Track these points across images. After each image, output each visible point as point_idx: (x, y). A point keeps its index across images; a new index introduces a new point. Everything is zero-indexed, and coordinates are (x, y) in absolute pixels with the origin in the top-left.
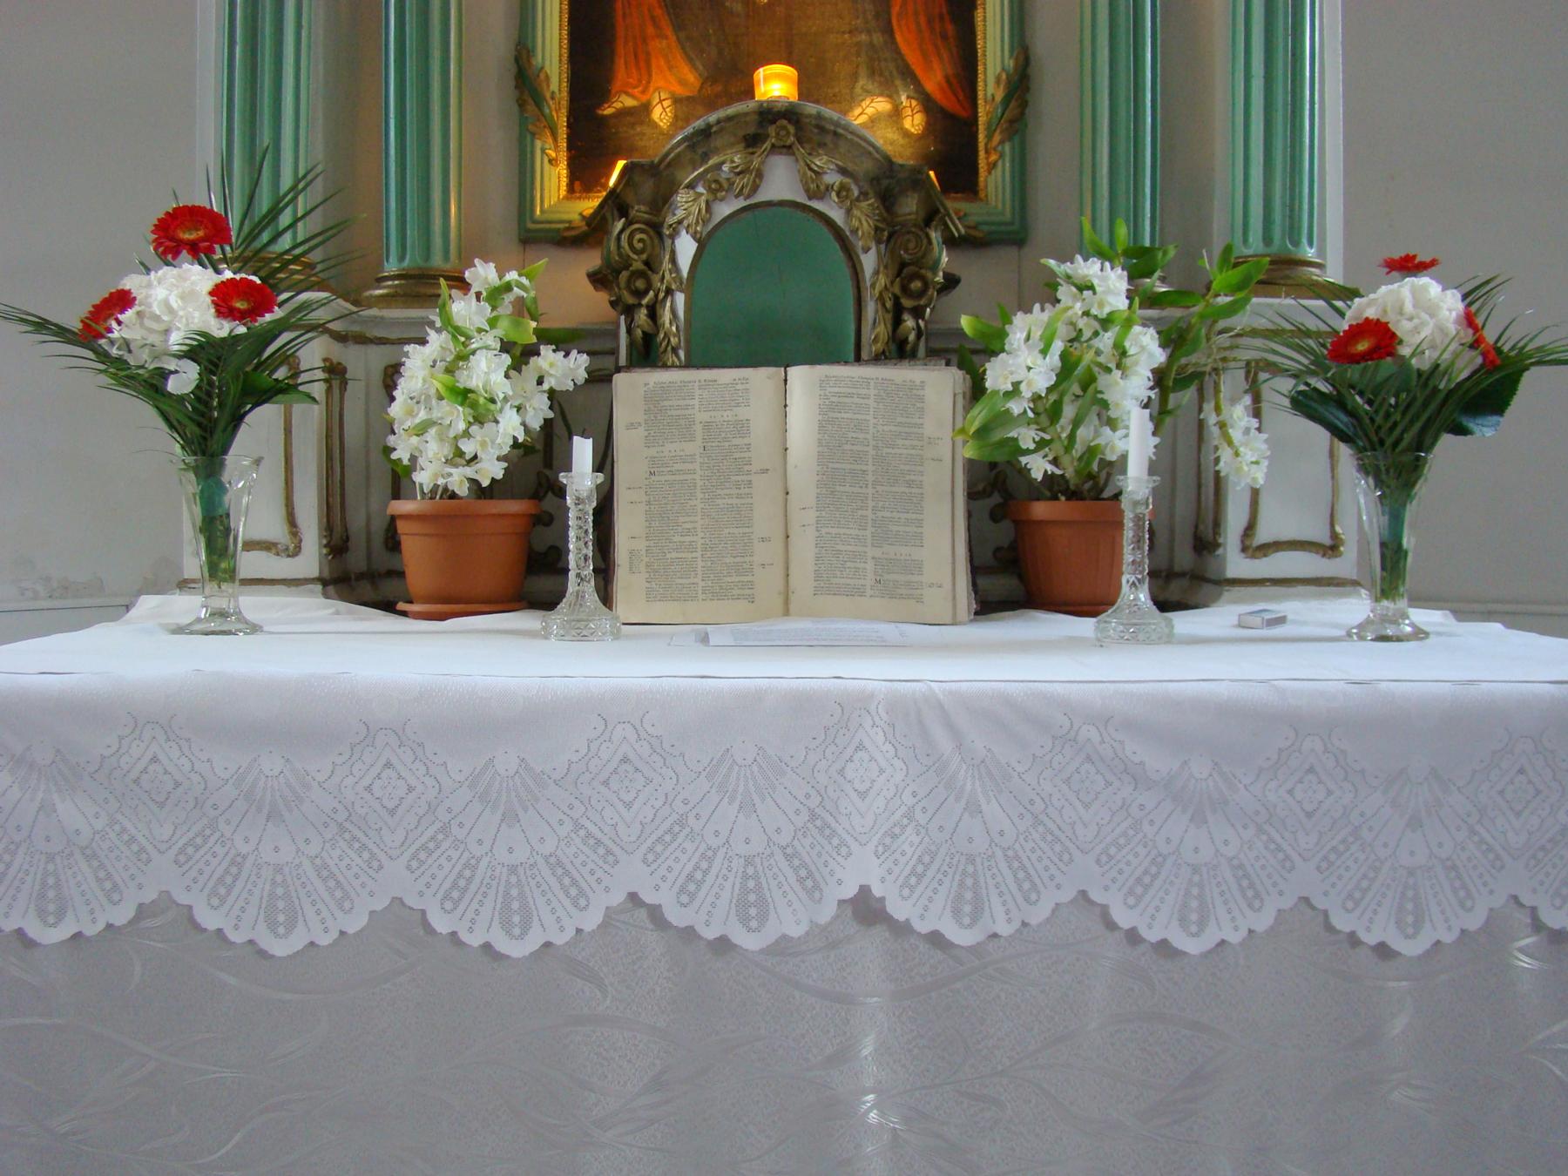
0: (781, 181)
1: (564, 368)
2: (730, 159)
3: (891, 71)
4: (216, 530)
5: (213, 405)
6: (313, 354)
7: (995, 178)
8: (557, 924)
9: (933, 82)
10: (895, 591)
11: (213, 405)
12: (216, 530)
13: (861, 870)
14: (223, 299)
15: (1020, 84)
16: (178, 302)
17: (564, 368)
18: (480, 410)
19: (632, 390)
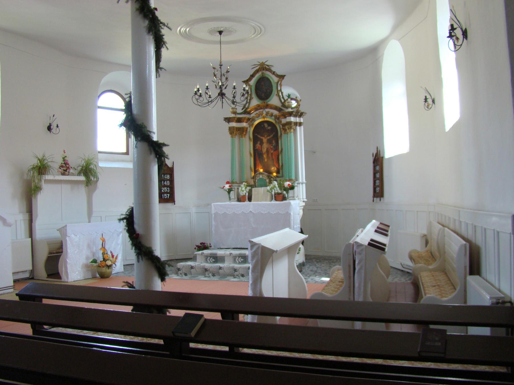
0: (261, 177)
1: (248, 188)
2: (258, 175)
3: (274, 166)
4: (230, 198)
5: (229, 191)
6: (236, 188)
7: (281, 172)
8: (240, 212)
9: (277, 166)
10: (266, 200)
11: (229, 191)
12: (230, 198)
13: (251, 210)
14: (230, 186)
15: (282, 165)
16: (227, 186)
17: (248, 188)
18: (243, 191)
19: (253, 189)
